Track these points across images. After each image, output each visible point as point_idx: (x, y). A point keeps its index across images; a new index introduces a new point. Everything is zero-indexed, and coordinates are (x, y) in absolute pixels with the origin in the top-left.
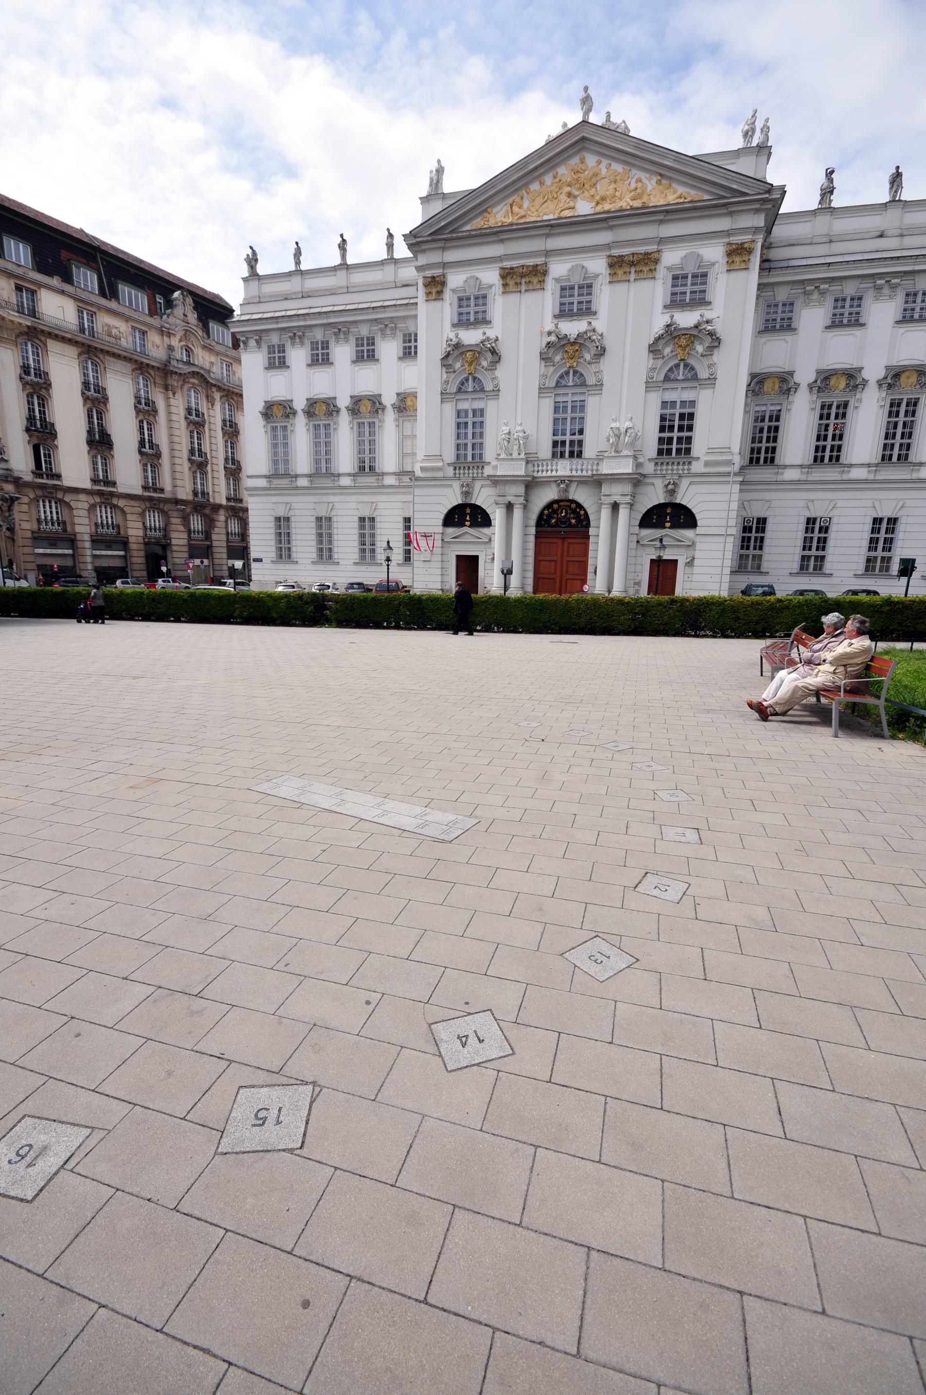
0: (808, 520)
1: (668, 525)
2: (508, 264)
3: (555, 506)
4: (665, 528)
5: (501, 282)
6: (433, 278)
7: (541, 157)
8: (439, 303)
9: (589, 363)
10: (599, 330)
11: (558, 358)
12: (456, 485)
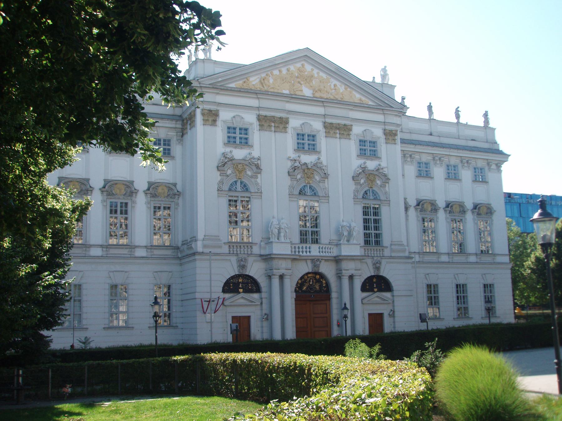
0: (428, 285)
1: (376, 290)
2: (263, 113)
3: (306, 277)
4: (375, 292)
5: (258, 123)
6: (210, 111)
7: (283, 59)
8: (213, 128)
9: (319, 182)
10: (325, 163)
11: (299, 177)
12: (234, 259)
